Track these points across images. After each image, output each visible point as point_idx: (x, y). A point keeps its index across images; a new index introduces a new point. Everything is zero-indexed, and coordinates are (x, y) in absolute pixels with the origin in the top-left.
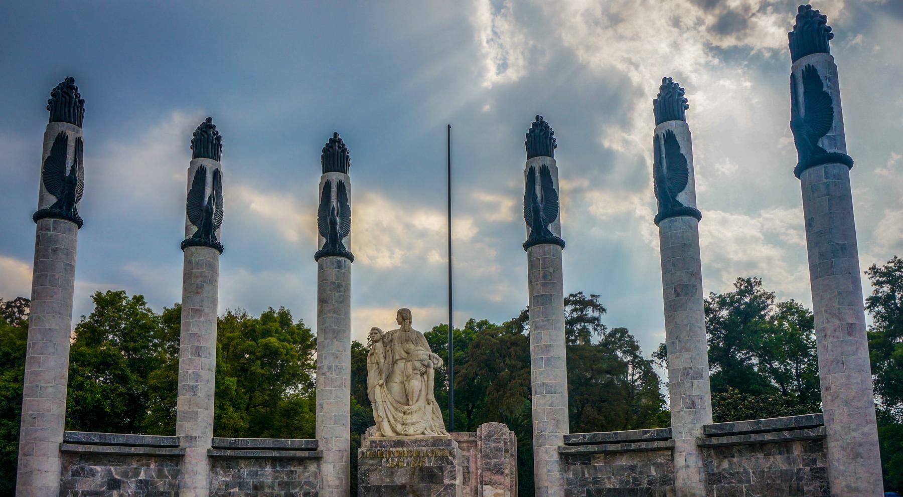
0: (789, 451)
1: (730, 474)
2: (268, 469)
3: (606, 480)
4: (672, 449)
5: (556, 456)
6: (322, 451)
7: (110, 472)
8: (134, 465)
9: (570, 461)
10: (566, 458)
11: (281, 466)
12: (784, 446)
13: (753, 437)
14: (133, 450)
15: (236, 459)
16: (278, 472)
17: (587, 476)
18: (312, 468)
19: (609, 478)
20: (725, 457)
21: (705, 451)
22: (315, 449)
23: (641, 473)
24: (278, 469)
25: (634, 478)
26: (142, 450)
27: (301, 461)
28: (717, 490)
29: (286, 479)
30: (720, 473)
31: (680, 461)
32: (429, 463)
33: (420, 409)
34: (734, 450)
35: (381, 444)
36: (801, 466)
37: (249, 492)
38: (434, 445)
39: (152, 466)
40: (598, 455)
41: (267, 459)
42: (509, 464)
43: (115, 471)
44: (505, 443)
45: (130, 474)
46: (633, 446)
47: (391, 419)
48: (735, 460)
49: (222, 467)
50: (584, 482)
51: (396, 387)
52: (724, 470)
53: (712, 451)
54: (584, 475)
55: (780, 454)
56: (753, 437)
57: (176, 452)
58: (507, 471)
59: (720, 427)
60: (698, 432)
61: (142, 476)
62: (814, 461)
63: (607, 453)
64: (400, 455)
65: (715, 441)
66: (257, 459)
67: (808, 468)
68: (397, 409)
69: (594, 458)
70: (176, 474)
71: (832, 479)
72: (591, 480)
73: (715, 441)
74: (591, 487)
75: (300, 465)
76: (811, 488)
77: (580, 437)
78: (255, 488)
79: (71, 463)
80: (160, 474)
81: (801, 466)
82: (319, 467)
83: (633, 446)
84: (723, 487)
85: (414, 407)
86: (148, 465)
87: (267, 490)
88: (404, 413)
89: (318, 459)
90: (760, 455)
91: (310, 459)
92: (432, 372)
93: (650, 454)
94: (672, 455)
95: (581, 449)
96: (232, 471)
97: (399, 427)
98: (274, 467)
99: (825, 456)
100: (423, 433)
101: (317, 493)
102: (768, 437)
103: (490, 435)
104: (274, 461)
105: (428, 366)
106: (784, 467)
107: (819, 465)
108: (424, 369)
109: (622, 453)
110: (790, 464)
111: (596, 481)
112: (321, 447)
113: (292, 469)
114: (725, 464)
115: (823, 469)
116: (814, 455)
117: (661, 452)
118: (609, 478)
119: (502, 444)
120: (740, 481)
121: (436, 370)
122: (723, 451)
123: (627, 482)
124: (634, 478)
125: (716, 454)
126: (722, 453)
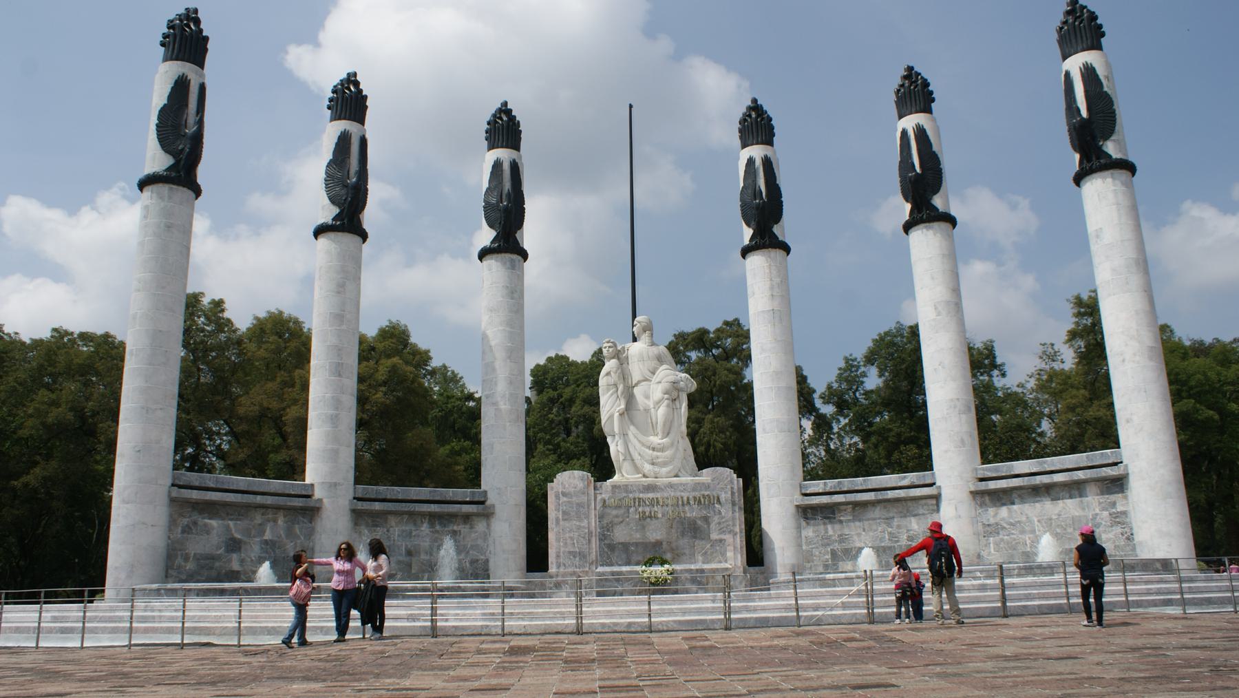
1: (1011, 524)
2: (425, 528)
3: (855, 538)
5: (792, 510)
6: (493, 506)
7: (228, 528)
8: (258, 519)
9: (809, 515)
10: (807, 513)
11: (440, 524)
12: (1075, 489)
13: (1038, 480)
14: (259, 499)
15: (384, 514)
16: (437, 532)
17: (831, 532)
18: (481, 526)
19: (859, 535)
20: (1004, 504)
21: (978, 498)
22: (483, 503)
23: (899, 527)
24: (438, 527)
25: (890, 533)
26: (269, 500)
27: (467, 518)
28: (996, 544)
30: (997, 524)
32: (692, 513)
33: (672, 444)
34: (1014, 495)
35: (626, 488)
36: (1097, 511)
37: (401, 558)
38: (694, 490)
39: (281, 521)
40: (843, 507)
41: (423, 515)
42: (739, 517)
43: (236, 528)
44: (733, 493)
45: (253, 532)
46: (891, 494)
47: (636, 456)
48: (1015, 507)
49: (367, 525)
50: (827, 540)
52: (1003, 519)
53: (987, 498)
54: (827, 532)
55: (1071, 497)
56: (1038, 480)
57: (310, 503)
59: (996, 470)
61: (268, 536)
62: (1114, 504)
63: (856, 505)
65: (992, 485)
66: (411, 514)
67: (1106, 513)
68: (643, 445)
69: (840, 511)
70: (310, 534)
71: (1134, 525)
72: (836, 538)
73: (992, 485)
74: (836, 546)
75: (465, 523)
76: (1111, 535)
77: (818, 486)
78: (409, 553)
79: (181, 515)
80: (290, 533)
81: (1097, 511)
82: (488, 525)
83: (891, 494)
84: (1002, 540)
86: (275, 521)
87: (423, 556)
88: (654, 449)
89: (488, 515)
91: (478, 515)
93: (909, 503)
94: (938, 505)
95: (825, 500)
97: (647, 468)
98: (432, 525)
99: (1126, 498)
100: (676, 476)
101: (487, 561)
102: (1059, 478)
104: (433, 517)
105: (679, 390)
106: (1077, 513)
107: (1120, 508)
108: (675, 394)
110: (1083, 509)
111: (842, 539)
112: (492, 499)
113: (455, 528)
114: (1004, 512)
115: (1124, 513)
116: (1113, 497)
117: (923, 502)
118: (859, 535)
120: (1023, 532)
121: (690, 396)
123: (882, 540)
124: (890, 533)
125: (992, 500)
126: (999, 499)
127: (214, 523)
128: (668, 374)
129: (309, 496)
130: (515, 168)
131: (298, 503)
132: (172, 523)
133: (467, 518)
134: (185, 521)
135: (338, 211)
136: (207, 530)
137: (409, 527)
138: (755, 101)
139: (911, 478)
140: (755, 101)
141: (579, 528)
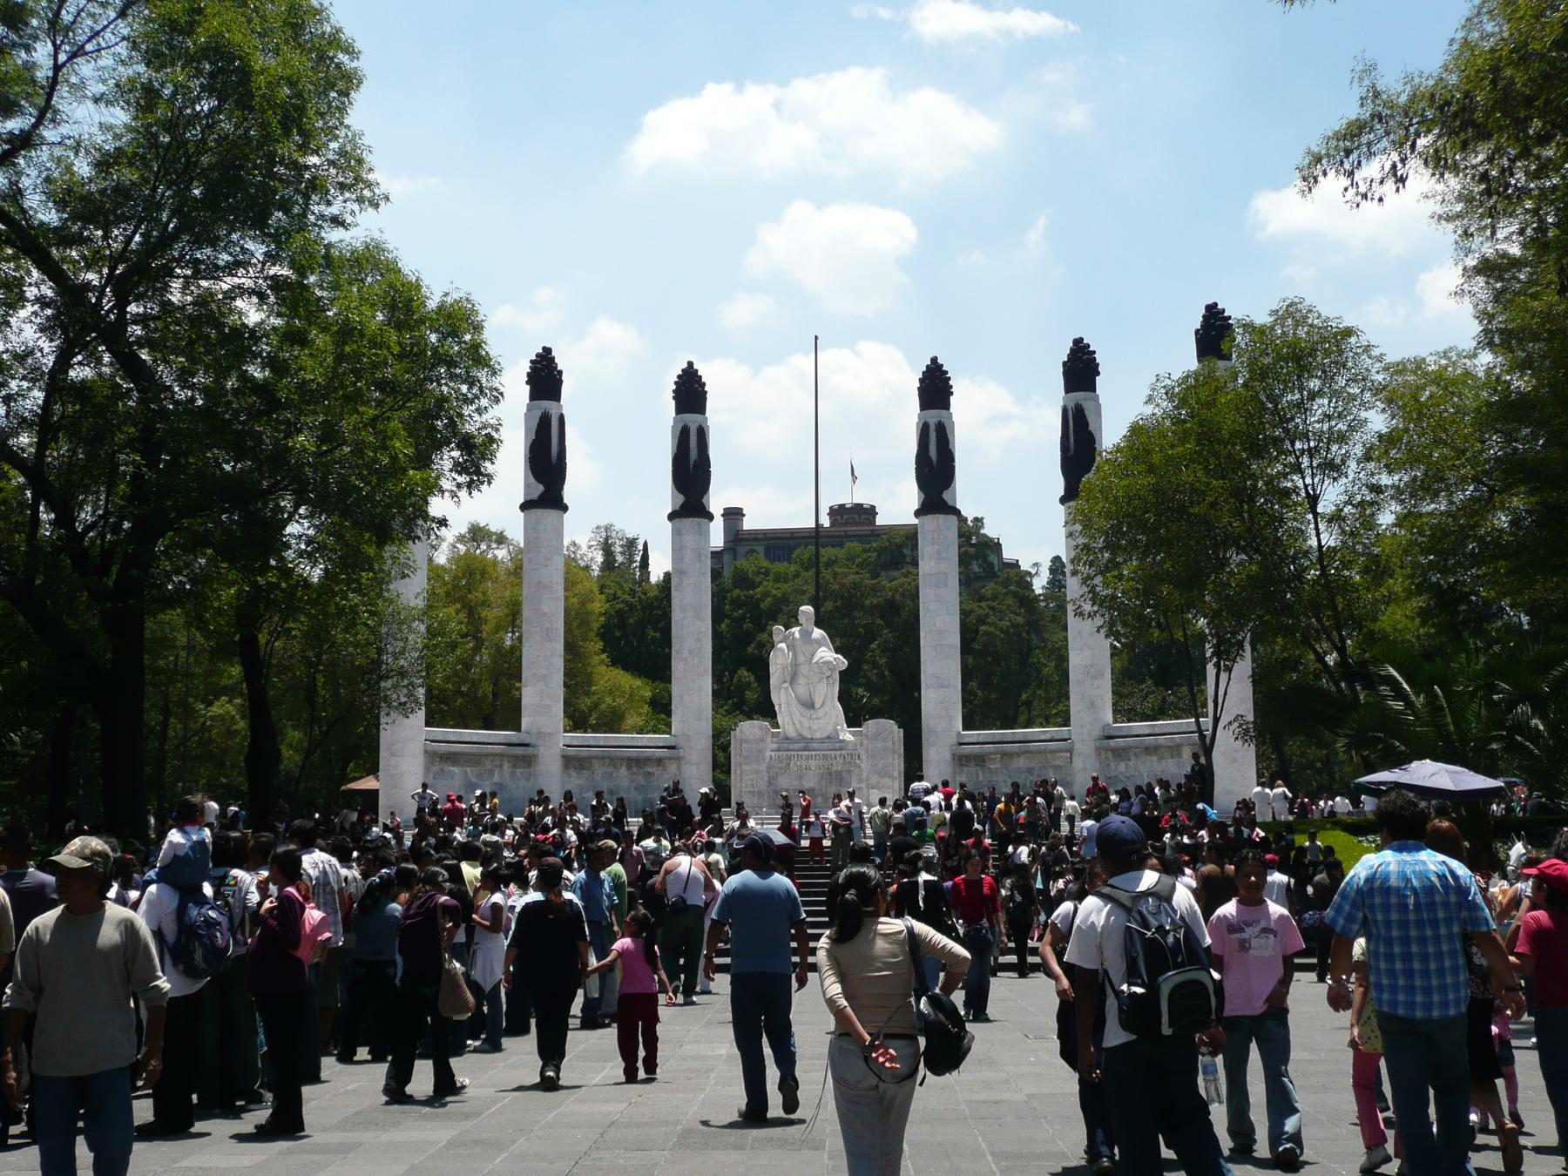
0: (1179, 755)
2: (623, 770)
4: (1070, 751)
5: (948, 757)
8: (489, 766)
29: (642, 782)
31: (1078, 763)
51: (801, 689)
57: (529, 751)
58: (896, 774)
60: (1097, 733)
64: (808, 758)
80: (512, 774)
82: (679, 768)
85: (821, 713)
90: (1155, 758)
92: (837, 677)
96: (586, 773)
98: (629, 768)
103: (876, 736)
109: (1018, 755)
114: (1122, 767)
119: (890, 744)
122: (1121, 754)
127: (456, 769)
128: (827, 654)
129: (527, 745)
130: (702, 433)
131: (519, 751)
132: (427, 769)
133: (660, 761)
134: (436, 768)
135: (541, 488)
136: (452, 775)
137: (609, 770)
138: (934, 360)
139: (1052, 730)
140: (934, 360)
141: (757, 772)
